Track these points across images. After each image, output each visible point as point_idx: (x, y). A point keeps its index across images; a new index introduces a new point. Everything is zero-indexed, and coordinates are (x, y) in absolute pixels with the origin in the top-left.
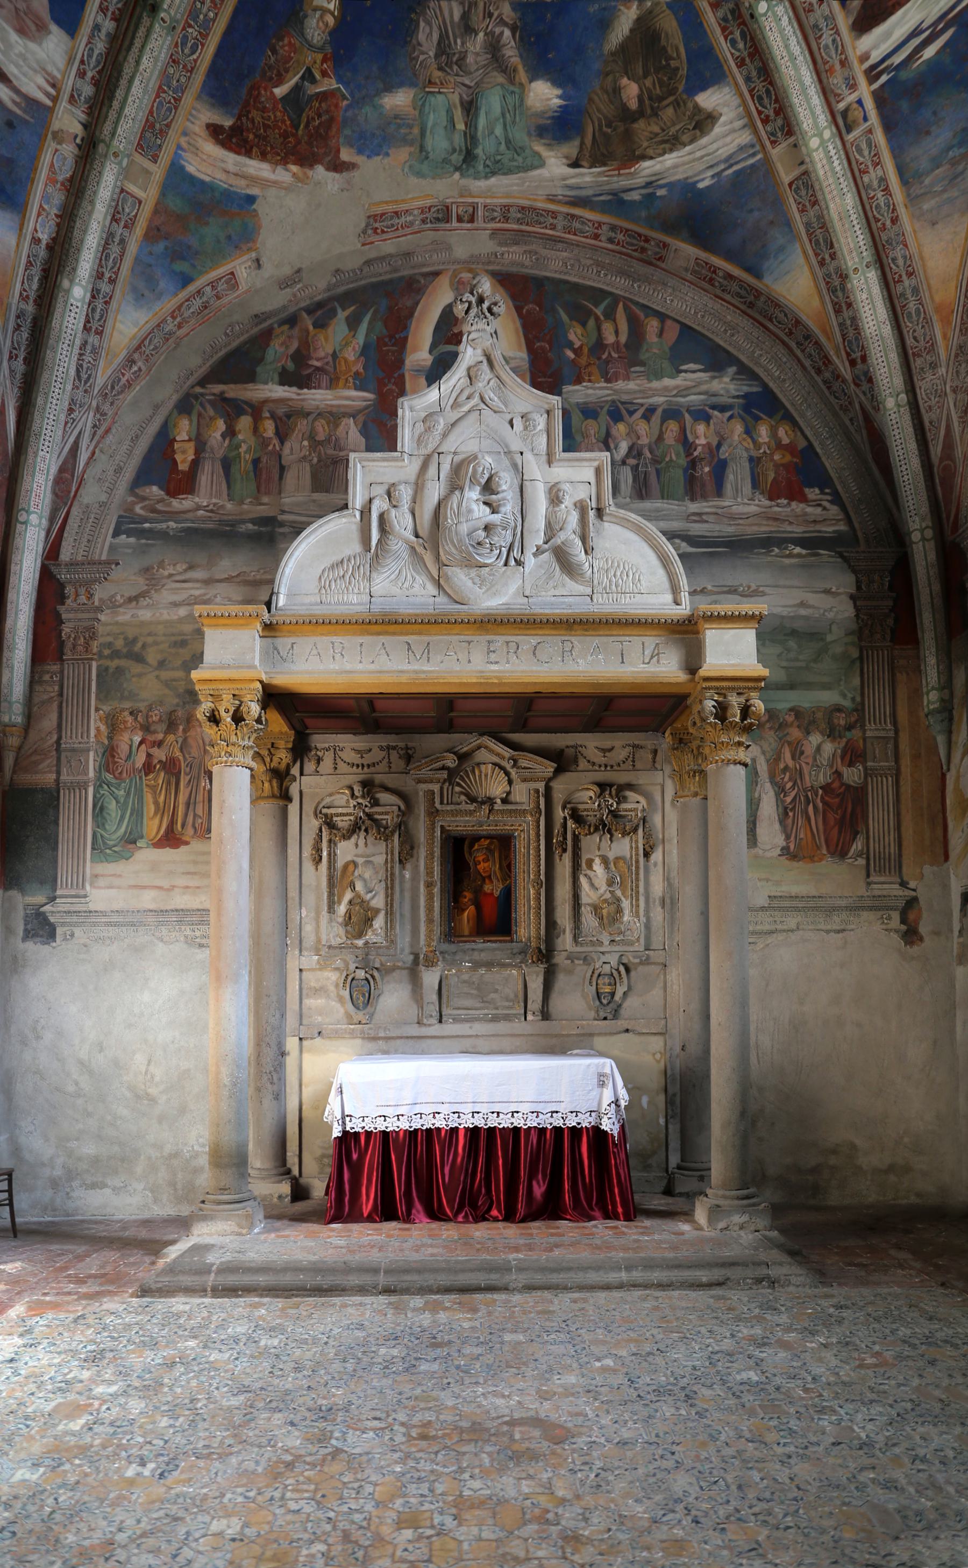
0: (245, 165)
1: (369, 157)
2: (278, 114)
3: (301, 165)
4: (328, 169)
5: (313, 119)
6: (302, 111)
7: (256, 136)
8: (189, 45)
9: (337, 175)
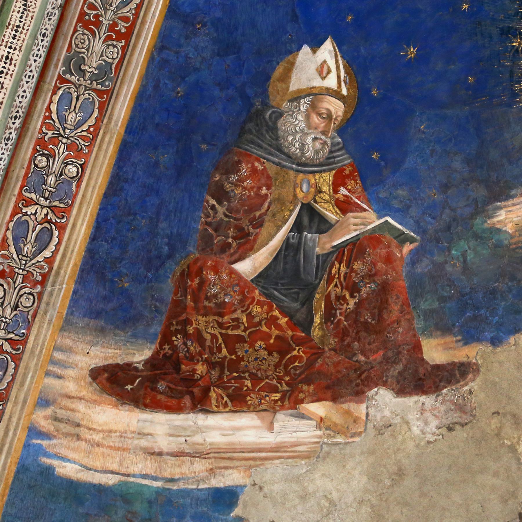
0: (199, 430)
1: (495, 342)
2: (257, 309)
3: (334, 399)
4: (401, 392)
5: (341, 298)
6: (315, 288)
7: (211, 365)
8: (32, 236)
9: (428, 400)
